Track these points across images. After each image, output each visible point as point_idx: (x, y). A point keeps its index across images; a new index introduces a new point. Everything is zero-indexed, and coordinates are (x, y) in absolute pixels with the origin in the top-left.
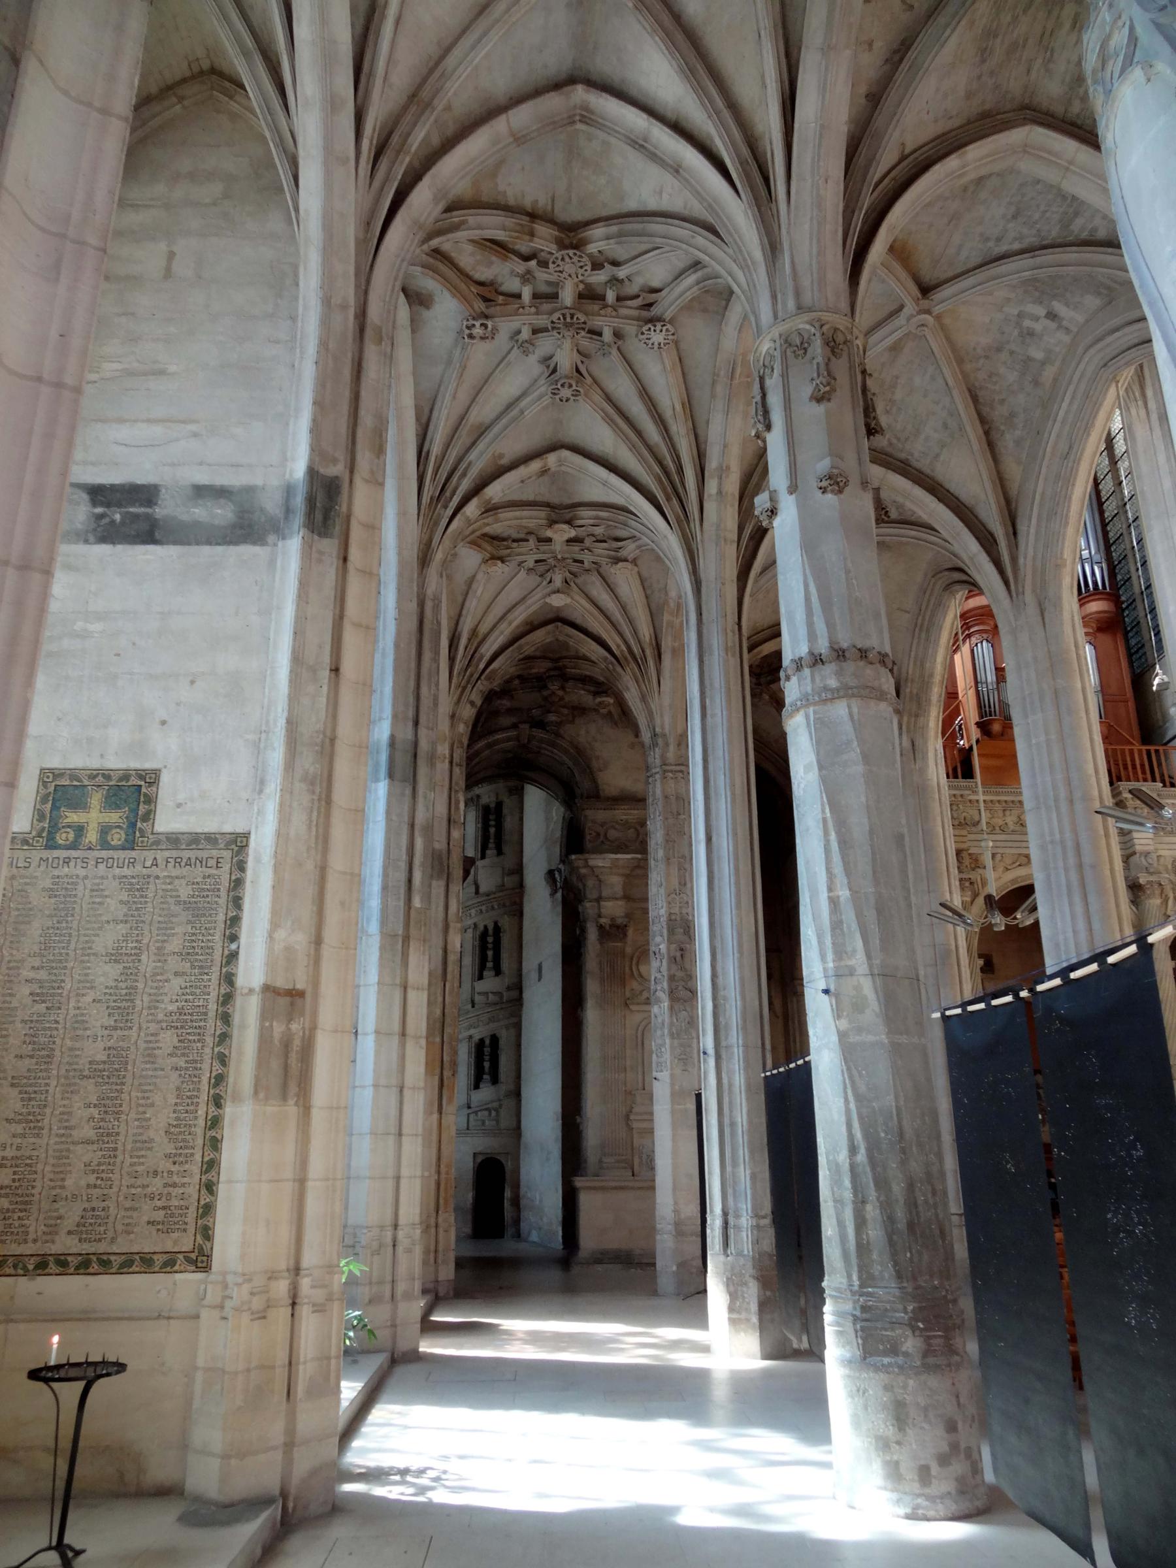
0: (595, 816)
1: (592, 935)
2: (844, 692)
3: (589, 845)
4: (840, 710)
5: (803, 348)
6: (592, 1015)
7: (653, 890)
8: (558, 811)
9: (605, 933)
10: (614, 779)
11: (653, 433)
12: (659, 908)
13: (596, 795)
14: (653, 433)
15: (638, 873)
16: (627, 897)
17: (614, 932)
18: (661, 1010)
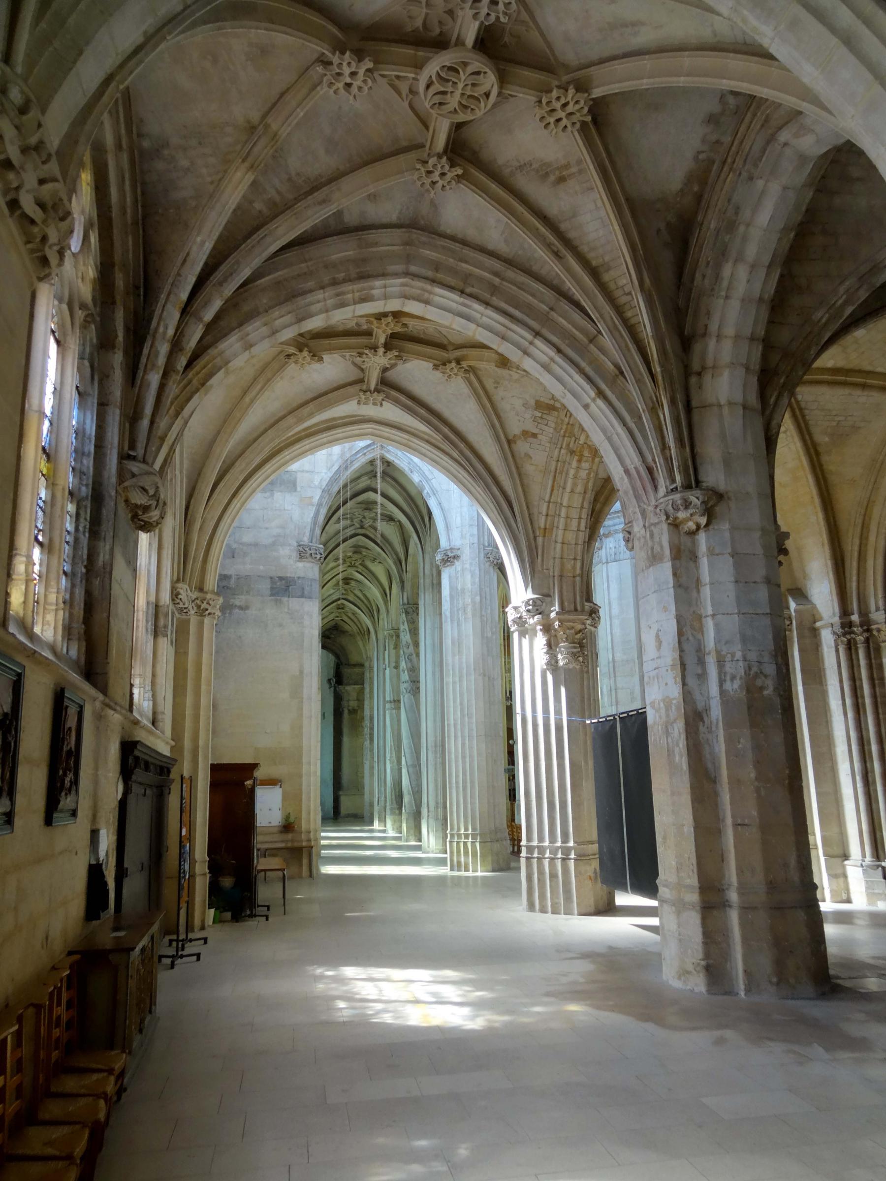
0: (346, 671)
1: (346, 712)
2: (395, 709)
3: (345, 681)
4: (394, 711)
5: (392, 637)
6: (346, 740)
7: (366, 706)
8: (332, 658)
9: (350, 712)
10: (354, 658)
11: (365, 601)
12: (367, 713)
13: (349, 665)
14: (365, 601)
15: (361, 692)
16: (358, 700)
17: (353, 712)
18: (367, 743)
